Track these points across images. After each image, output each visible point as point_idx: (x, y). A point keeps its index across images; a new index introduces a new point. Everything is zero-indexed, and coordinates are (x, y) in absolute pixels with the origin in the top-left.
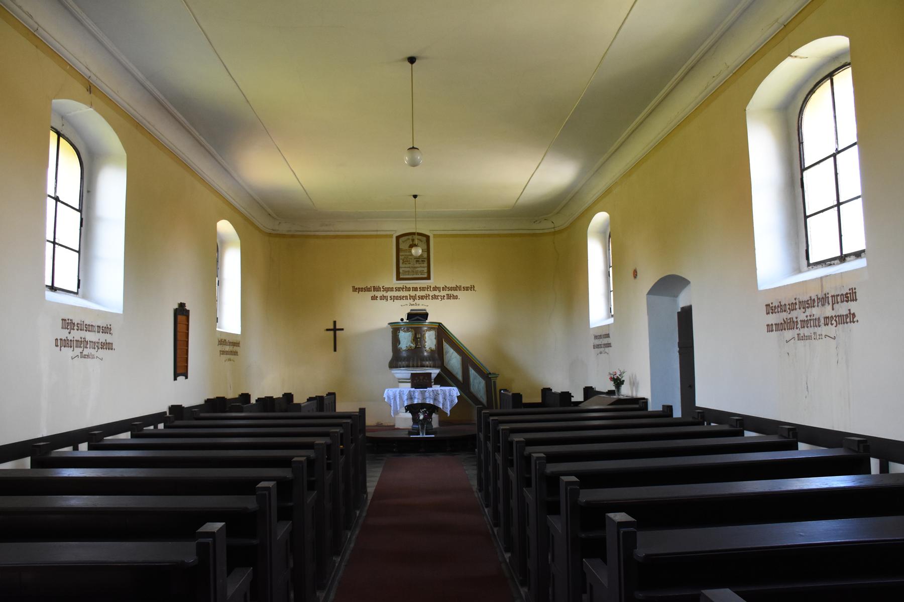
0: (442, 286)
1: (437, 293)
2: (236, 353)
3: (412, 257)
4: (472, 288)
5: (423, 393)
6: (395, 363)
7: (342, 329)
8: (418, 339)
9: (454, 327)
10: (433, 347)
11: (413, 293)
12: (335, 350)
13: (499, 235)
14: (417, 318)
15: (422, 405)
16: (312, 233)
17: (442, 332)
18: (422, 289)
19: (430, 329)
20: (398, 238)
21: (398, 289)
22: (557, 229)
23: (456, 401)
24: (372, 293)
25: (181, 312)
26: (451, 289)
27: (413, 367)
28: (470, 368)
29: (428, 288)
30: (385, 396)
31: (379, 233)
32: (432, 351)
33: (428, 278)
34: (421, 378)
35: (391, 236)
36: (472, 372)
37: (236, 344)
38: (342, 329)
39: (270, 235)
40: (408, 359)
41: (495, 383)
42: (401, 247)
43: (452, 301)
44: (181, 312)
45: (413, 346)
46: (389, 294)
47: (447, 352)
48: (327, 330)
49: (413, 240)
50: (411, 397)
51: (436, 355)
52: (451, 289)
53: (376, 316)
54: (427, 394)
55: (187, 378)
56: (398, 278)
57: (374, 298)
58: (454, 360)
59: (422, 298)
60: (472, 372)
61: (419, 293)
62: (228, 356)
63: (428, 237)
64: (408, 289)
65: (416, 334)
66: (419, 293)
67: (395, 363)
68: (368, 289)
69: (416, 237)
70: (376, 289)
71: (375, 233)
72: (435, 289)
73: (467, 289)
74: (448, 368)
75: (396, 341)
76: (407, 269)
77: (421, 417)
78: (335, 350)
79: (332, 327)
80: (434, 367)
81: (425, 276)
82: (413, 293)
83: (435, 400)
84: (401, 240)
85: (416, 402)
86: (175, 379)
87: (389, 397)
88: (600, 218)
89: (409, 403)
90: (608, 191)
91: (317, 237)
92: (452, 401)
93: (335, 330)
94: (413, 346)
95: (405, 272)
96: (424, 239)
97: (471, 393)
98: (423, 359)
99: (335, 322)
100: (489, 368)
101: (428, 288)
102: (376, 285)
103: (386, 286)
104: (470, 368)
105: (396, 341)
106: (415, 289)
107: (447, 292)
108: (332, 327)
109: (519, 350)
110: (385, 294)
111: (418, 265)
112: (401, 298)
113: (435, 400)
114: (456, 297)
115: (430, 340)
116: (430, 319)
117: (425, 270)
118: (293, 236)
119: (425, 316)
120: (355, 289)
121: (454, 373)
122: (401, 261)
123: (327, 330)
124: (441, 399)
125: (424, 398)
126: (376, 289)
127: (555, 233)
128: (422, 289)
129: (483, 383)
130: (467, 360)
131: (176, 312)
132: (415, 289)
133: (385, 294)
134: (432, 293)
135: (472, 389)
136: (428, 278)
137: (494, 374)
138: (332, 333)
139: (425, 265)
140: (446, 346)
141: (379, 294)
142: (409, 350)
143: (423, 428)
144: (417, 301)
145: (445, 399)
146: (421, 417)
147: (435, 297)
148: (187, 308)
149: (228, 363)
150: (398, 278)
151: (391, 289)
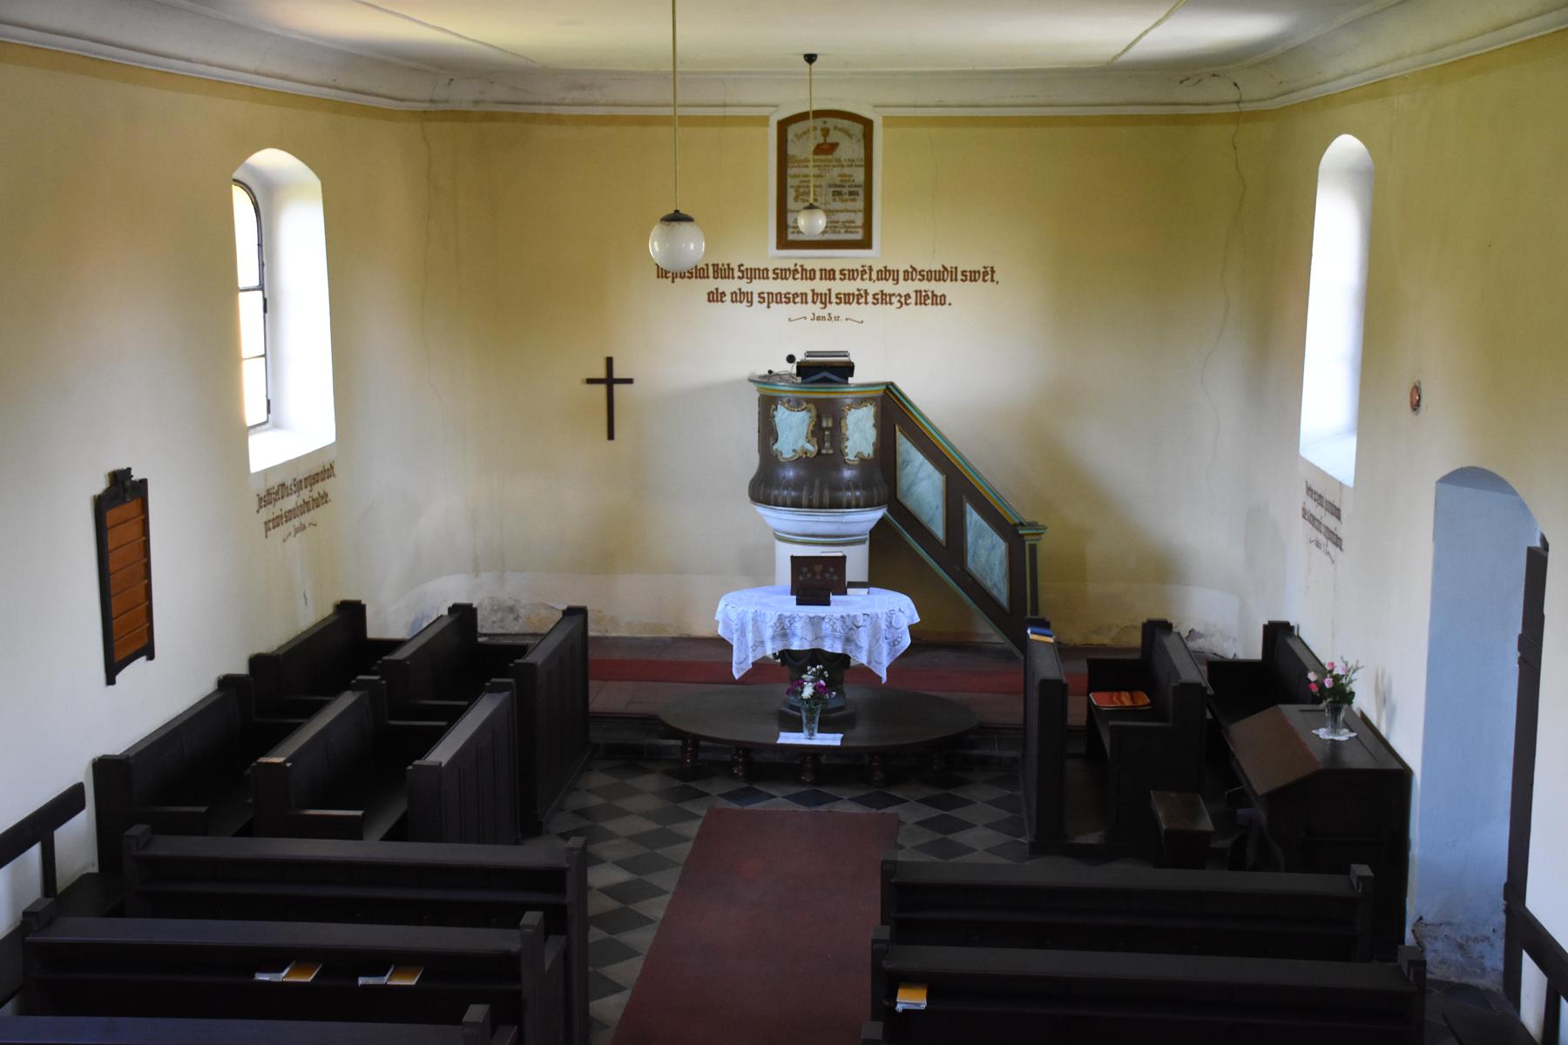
0: (903, 267)
1: (888, 286)
2: (323, 499)
3: (826, 165)
4: (988, 274)
5: (815, 622)
7: (630, 381)
8: (827, 427)
9: (927, 394)
10: (868, 450)
11: (821, 286)
12: (611, 436)
13: (1072, 121)
15: (816, 656)
17: (892, 408)
18: (849, 275)
19: (860, 402)
20: (783, 125)
21: (781, 274)
22: (1246, 107)
23: (906, 641)
24: (712, 284)
25: (123, 498)
27: (810, 506)
28: (969, 508)
29: (864, 272)
30: (719, 616)
31: (730, 112)
32: (863, 462)
34: (818, 568)
35: (764, 121)
36: (973, 518)
37: (327, 473)
38: (630, 381)
39: (425, 116)
40: (797, 485)
41: (1033, 548)
42: (792, 150)
43: (930, 310)
44: (123, 498)
45: (812, 448)
46: (758, 286)
47: (907, 463)
48: (590, 381)
49: (826, 132)
50: (783, 632)
53: (722, 348)
54: (826, 626)
55: (151, 657)
56: (783, 242)
57: (715, 297)
58: (923, 485)
59: (846, 299)
60: (973, 518)
61: (840, 286)
62: (296, 522)
63: (868, 124)
64: (809, 275)
65: (819, 418)
66: (840, 286)
68: (698, 273)
69: (831, 122)
70: (723, 272)
71: (719, 112)
72: (885, 274)
73: (972, 276)
74: (910, 503)
75: (768, 432)
77: (808, 691)
78: (611, 436)
79: (602, 374)
80: (869, 504)
81: (859, 236)
82: (821, 286)
83: (848, 640)
84: (793, 130)
85: (795, 645)
86: (111, 681)
87: (727, 626)
88: (1345, 148)
89: (779, 647)
90: (1378, 89)
91: (558, 120)
92: (894, 643)
93: (610, 381)
94: (812, 448)
96: (857, 128)
97: (968, 574)
99: (609, 361)
100: (1020, 508)
101: (864, 272)
102: (721, 260)
103: (747, 265)
104: (969, 508)
105: (768, 432)
106: (829, 275)
107: (918, 285)
108: (602, 374)
109: (1108, 452)
110: (744, 285)
111: (839, 205)
112: (789, 298)
113: (848, 640)
114: (940, 300)
115: (860, 432)
116: (856, 379)
117: (859, 219)
118: (490, 117)
119: (847, 369)
121: (924, 519)
122: (791, 194)
123: (590, 381)
124: (863, 638)
126: (723, 272)
127: (1237, 118)
128: (849, 275)
129: (1001, 547)
130: (961, 488)
131: (102, 505)
132: (829, 275)
133: (744, 285)
134: (874, 287)
135: (971, 565)
136: (866, 243)
137: (1032, 525)
138: (602, 388)
139: (859, 204)
140: (905, 446)
141: (728, 286)
142: (802, 461)
143: (811, 720)
144: (833, 309)
146: (808, 691)
147: (883, 298)
148: (137, 476)
149: (293, 542)
150: (783, 242)
151: (762, 274)
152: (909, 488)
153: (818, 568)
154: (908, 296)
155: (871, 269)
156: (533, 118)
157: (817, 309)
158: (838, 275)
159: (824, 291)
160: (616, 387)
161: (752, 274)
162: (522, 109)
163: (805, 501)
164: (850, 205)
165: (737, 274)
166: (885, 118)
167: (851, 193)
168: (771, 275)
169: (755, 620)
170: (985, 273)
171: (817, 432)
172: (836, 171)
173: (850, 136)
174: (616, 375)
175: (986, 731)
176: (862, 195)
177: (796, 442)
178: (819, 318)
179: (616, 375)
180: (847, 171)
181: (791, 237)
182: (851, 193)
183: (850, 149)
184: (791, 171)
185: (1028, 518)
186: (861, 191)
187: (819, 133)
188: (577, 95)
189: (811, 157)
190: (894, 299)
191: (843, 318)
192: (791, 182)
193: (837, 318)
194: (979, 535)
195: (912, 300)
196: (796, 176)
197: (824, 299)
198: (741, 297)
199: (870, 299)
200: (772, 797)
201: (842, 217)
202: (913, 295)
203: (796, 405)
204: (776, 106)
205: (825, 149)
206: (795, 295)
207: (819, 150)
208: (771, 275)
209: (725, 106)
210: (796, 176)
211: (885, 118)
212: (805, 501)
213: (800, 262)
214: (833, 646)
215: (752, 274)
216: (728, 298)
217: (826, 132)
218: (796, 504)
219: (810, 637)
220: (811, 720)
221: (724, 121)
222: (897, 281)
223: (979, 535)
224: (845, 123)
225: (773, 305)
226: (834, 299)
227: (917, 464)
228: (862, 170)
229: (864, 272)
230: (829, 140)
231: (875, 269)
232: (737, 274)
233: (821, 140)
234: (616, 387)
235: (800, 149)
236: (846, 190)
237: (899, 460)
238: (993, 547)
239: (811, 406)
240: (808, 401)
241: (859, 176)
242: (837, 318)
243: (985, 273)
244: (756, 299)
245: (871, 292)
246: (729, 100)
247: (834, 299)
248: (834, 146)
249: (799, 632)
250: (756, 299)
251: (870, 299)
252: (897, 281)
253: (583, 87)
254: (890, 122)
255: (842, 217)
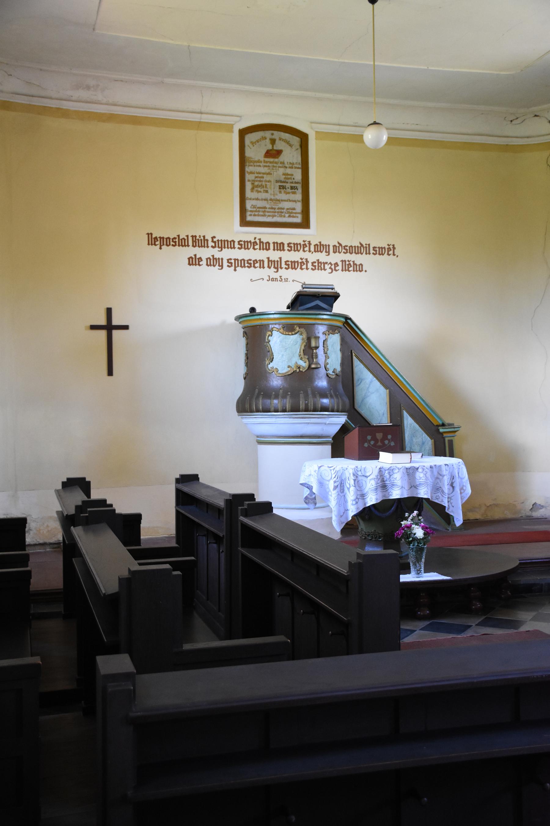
0: (332, 242)
1: (322, 257)
4: (390, 250)
6: (255, 397)
7: (126, 327)
10: (339, 369)
11: (274, 255)
12: (110, 372)
14: (312, 302)
16: (53, 104)
18: (294, 247)
20: (243, 133)
21: (244, 245)
24: (191, 251)
26: (350, 250)
27: (307, 410)
29: (304, 246)
31: (205, 118)
33: (305, 224)
35: (229, 128)
38: (126, 327)
41: (451, 442)
42: (249, 153)
43: (352, 275)
45: (304, 364)
46: (226, 254)
48: (93, 327)
49: (273, 141)
51: (340, 387)
52: (350, 250)
54: (420, 475)
56: (244, 222)
57: (194, 261)
59: (292, 265)
63: (303, 138)
64: (265, 246)
65: (309, 339)
67: (255, 397)
68: (180, 242)
69: (277, 134)
71: (196, 118)
72: (320, 247)
73: (380, 251)
74: (364, 412)
76: (260, 204)
78: (110, 372)
79: (103, 322)
81: (298, 219)
82: (274, 255)
85: (396, 494)
91: (65, 114)
93: (109, 328)
94: (304, 364)
95: (257, 210)
96: (295, 140)
98: (268, 393)
99: (109, 311)
101: (304, 246)
102: (199, 233)
103: (218, 237)
104: (405, 414)
106: (279, 247)
108: (103, 322)
111: (283, 196)
112: (250, 264)
114: (359, 268)
116: (338, 307)
117: (299, 207)
120: (152, 240)
122: (248, 186)
123: (93, 327)
125: (413, 486)
128: (294, 247)
132: (279, 247)
134: (312, 257)
136: (305, 224)
138: (103, 334)
139: (298, 196)
140: (358, 366)
141: (204, 253)
144: (283, 272)
145: (452, 485)
150: (244, 222)
151: (230, 244)
152: (363, 401)
153: (379, 436)
154: (336, 264)
155: (310, 243)
156: (44, 111)
157: (271, 272)
158: (286, 248)
159: (277, 259)
160: (115, 333)
161: (222, 244)
162: (36, 102)
163: (302, 406)
164: (292, 197)
165: (211, 244)
166: (317, 132)
167: (292, 188)
168: (237, 245)
169: (355, 475)
170: (389, 249)
171: (309, 351)
172: (281, 171)
173: (291, 146)
174: (115, 322)
175: (526, 566)
176: (300, 190)
177: (290, 360)
178: (273, 280)
179: (115, 322)
180: (289, 171)
181: (249, 218)
182: (292, 188)
183: (291, 155)
184: (247, 169)
185: (447, 421)
186: (299, 186)
187: (268, 141)
188: (83, 94)
189: (262, 159)
190: (327, 267)
191: (290, 279)
192: (248, 177)
193: (286, 280)
194: (413, 435)
195: (340, 268)
196: (251, 173)
197: (276, 265)
198: (213, 262)
199: (310, 265)
200: (413, 631)
201: (286, 205)
202: (340, 264)
203: (289, 329)
204: (240, 117)
205: (273, 154)
206: (255, 261)
207: (268, 154)
208: (237, 245)
209: (201, 113)
210: (251, 173)
211: (317, 132)
212: (302, 406)
213: (258, 237)
214: (423, 493)
215: (222, 244)
216: (204, 262)
217: (273, 141)
218: (295, 409)
219: (407, 487)
220: (418, 560)
221: (199, 126)
222: (328, 253)
223: (413, 435)
224: (286, 136)
225: (238, 269)
226: (284, 265)
227: (368, 381)
228: (300, 171)
229: (305, 246)
230: (275, 148)
231: (313, 244)
232: (211, 244)
233: (270, 147)
234: (115, 333)
235: (256, 152)
236: (288, 185)
237: (356, 377)
238: (423, 443)
239: (302, 330)
240: (301, 325)
241: (298, 175)
242: (286, 280)
243: (389, 249)
244: (225, 264)
245: (311, 261)
246: (203, 110)
247: (284, 265)
248: (279, 153)
249: (398, 482)
250: (225, 264)
251: (310, 265)
252: (328, 253)
253: (88, 88)
254: (320, 135)
255: (286, 205)
